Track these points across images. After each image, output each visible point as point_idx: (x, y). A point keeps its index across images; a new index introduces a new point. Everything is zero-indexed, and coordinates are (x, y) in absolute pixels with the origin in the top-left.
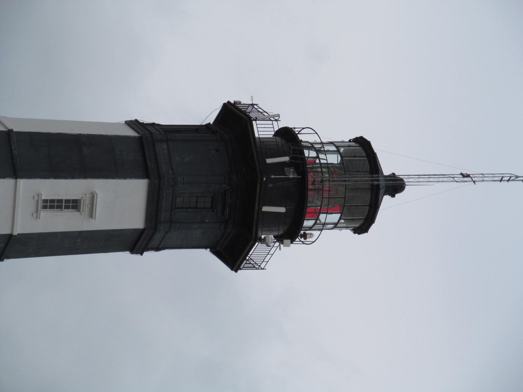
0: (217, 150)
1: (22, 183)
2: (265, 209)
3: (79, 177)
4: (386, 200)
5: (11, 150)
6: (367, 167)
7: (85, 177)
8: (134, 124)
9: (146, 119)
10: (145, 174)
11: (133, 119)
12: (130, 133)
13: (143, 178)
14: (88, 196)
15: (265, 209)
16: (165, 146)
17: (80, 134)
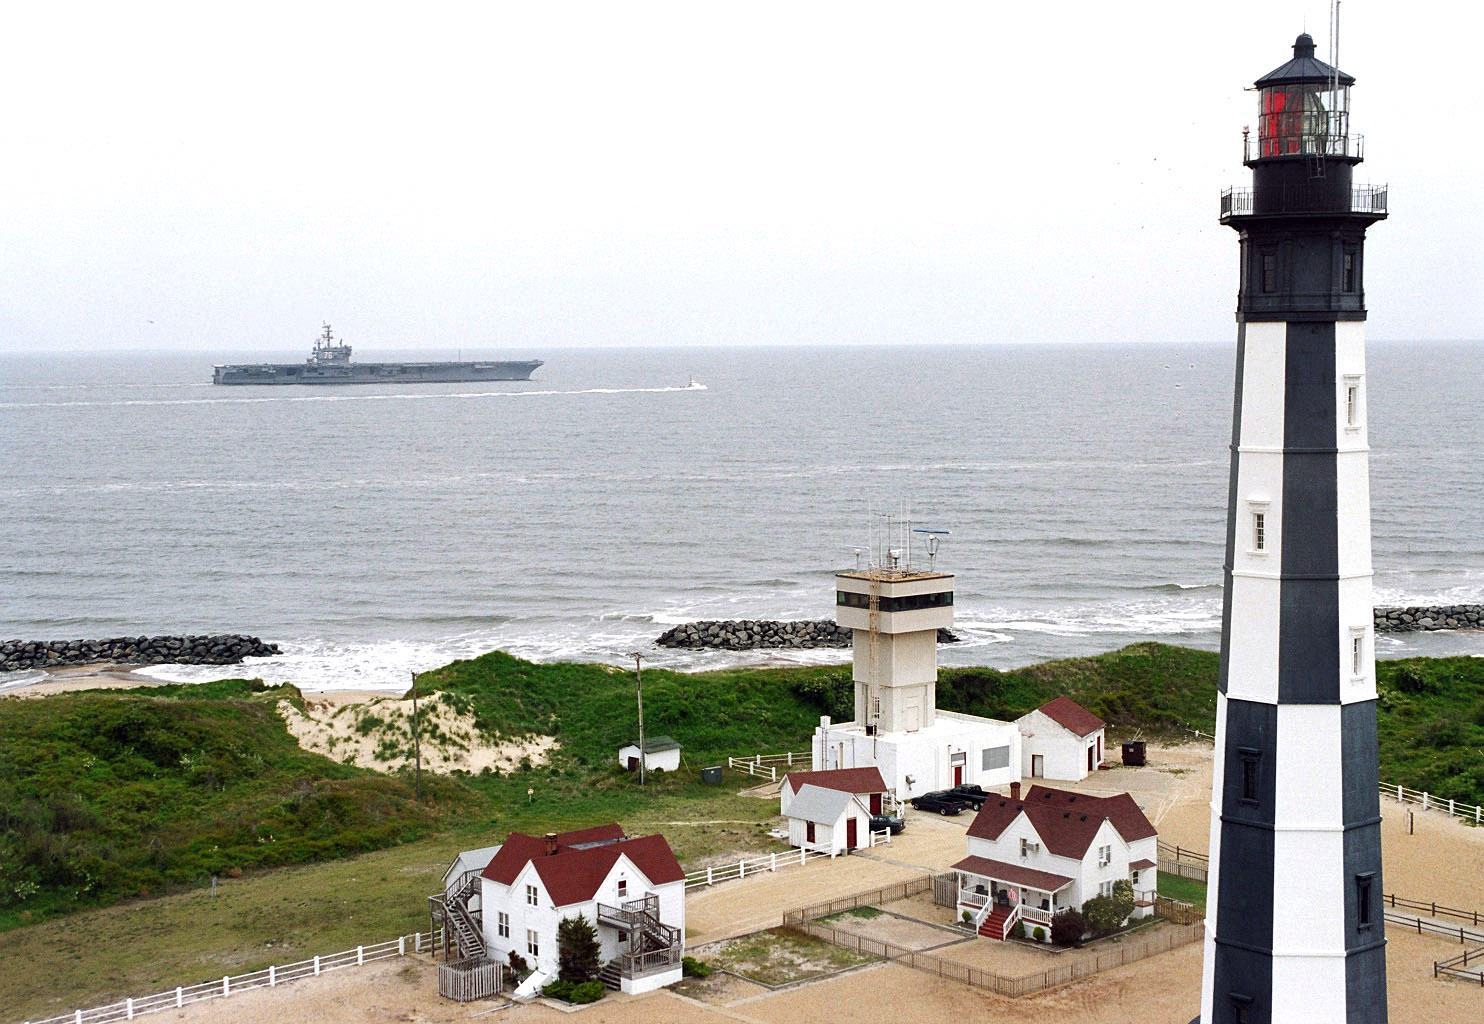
4: (1321, 54)
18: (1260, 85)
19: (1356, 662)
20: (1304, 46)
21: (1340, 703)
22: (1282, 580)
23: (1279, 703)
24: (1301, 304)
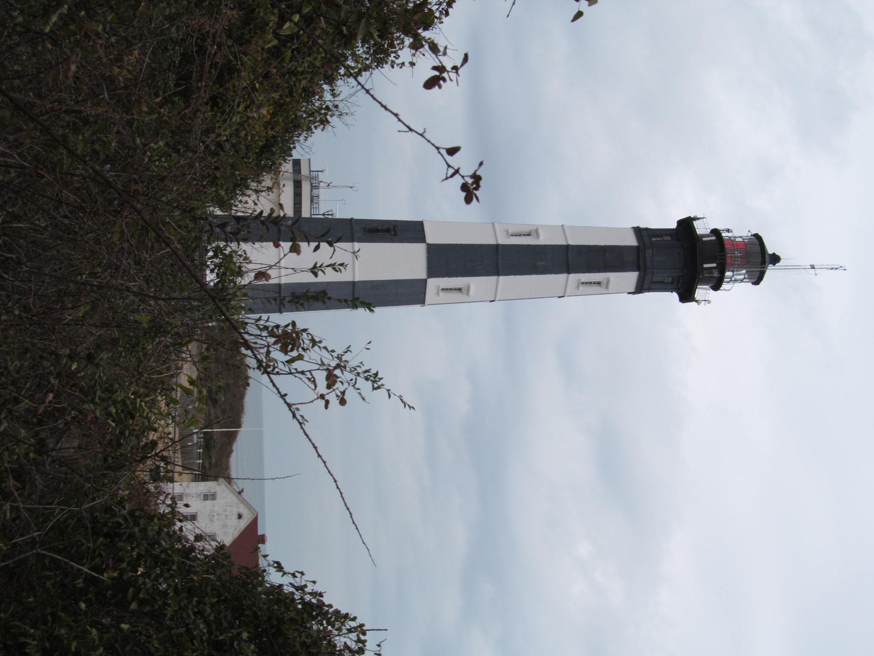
0: (679, 253)
2: (705, 266)
3: (602, 272)
4: (771, 267)
5: (568, 257)
6: (760, 260)
7: (605, 272)
8: (638, 231)
9: (642, 226)
10: (637, 268)
11: (636, 226)
12: (632, 241)
14: (606, 280)
15: (705, 266)
16: (651, 251)
17: (606, 246)
18: (757, 237)
19: (447, 289)
20: (775, 259)
22: (497, 246)
23: (428, 244)
24: (649, 252)
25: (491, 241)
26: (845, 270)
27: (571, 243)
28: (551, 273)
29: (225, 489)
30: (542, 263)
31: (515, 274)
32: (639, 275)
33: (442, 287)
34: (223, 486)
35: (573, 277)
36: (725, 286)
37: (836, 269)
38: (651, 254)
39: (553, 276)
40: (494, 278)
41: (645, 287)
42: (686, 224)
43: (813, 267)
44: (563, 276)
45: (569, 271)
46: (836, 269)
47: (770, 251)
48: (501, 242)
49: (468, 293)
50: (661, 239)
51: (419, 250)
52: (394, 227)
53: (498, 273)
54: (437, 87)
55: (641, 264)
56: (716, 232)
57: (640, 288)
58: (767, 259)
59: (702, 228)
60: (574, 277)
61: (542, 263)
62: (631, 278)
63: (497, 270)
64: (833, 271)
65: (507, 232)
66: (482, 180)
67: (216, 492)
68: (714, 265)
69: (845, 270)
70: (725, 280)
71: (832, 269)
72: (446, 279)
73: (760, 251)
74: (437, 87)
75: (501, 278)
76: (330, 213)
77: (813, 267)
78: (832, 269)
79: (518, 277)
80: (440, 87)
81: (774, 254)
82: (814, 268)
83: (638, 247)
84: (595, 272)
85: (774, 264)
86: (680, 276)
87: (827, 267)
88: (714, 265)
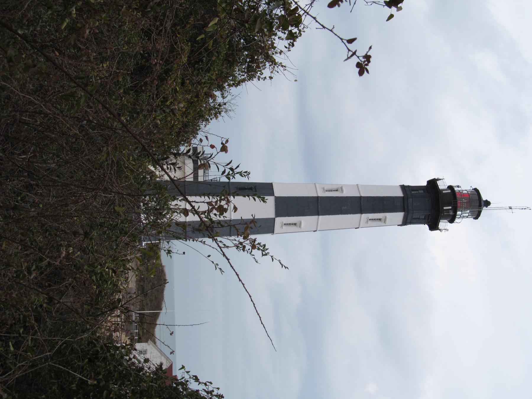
0: (428, 201)
1: (363, 215)
2: (445, 208)
4: (485, 208)
5: (361, 203)
7: (384, 212)
8: (403, 188)
9: (406, 184)
10: (404, 210)
11: (402, 184)
12: (400, 194)
13: (403, 212)
14: (384, 218)
15: (445, 208)
16: (411, 200)
18: (476, 190)
19: (287, 224)
20: (487, 203)
21: (276, 217)
22: (318, 198)
24: (410, 200)
25: (314, 195)
26: (530, 209)
27: (363, 195)
28: (351, 214)
29: (153, 347)
30: (345, 208)
31: (329, 215)
32: (404, 214)
33: (284, 223)
34: (151, 346)
35: (364, 215)
36: (457, 220)
37: (525, 209)
38: (411, 202)
39: (352, 215)
40: (316, 217)
41: (408, 221)
42: (433, 183)
43: (510, 208)
44: (358, 215)
45: (361, 212)
46: (525, 209)
47: (484, 198)
48: (320, 195)
49: (300, 227)
50: (417, 192)
51: (270, 200)
52: (255, 187)
53: (318, 214)
54: (337, 6)
55: (406, 207)
56: (451, 188)
57: (405, 222)
58: (483, 203)
59: (442, 185)
60: (365, 216)
61: (345, 208)
62: (400, 216)
63: (318, 213)
64: (523, 210)
65: (324, 189)
66: (372, 58)
67: (147, 350)
68: (450, 207)
69: (530, 209)
70: (457, 216)
71: (522, 209)
72: (287, 218)
73: (478, 199)
74: (337, 6)
75: (320, 217)
76: (216, 179)
77: (510, 208)
78: (522, 209)
79: (331, 216)
80: (339, 6)
81: (487, 201)
82: (511, 208)
83: (403, 197)
84: (377, 213)
85: (487, 207)
86: (430, 214)
87: (519, 208)
88: (450, 207)
